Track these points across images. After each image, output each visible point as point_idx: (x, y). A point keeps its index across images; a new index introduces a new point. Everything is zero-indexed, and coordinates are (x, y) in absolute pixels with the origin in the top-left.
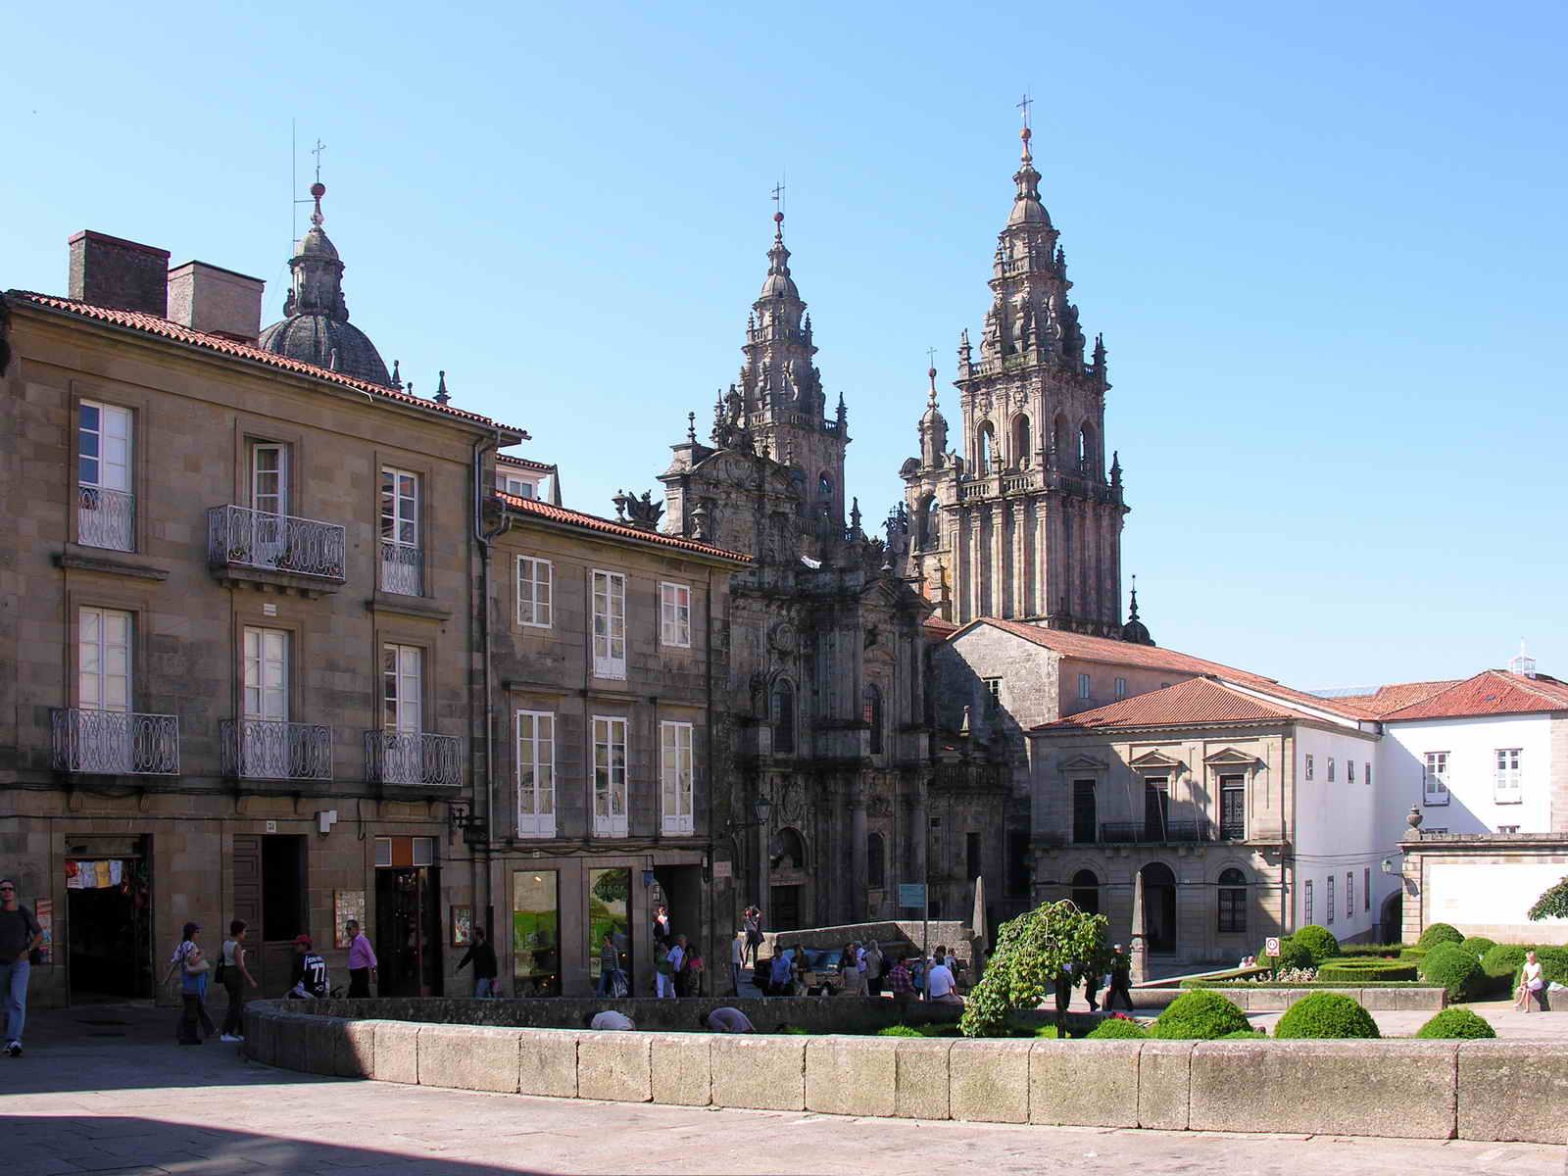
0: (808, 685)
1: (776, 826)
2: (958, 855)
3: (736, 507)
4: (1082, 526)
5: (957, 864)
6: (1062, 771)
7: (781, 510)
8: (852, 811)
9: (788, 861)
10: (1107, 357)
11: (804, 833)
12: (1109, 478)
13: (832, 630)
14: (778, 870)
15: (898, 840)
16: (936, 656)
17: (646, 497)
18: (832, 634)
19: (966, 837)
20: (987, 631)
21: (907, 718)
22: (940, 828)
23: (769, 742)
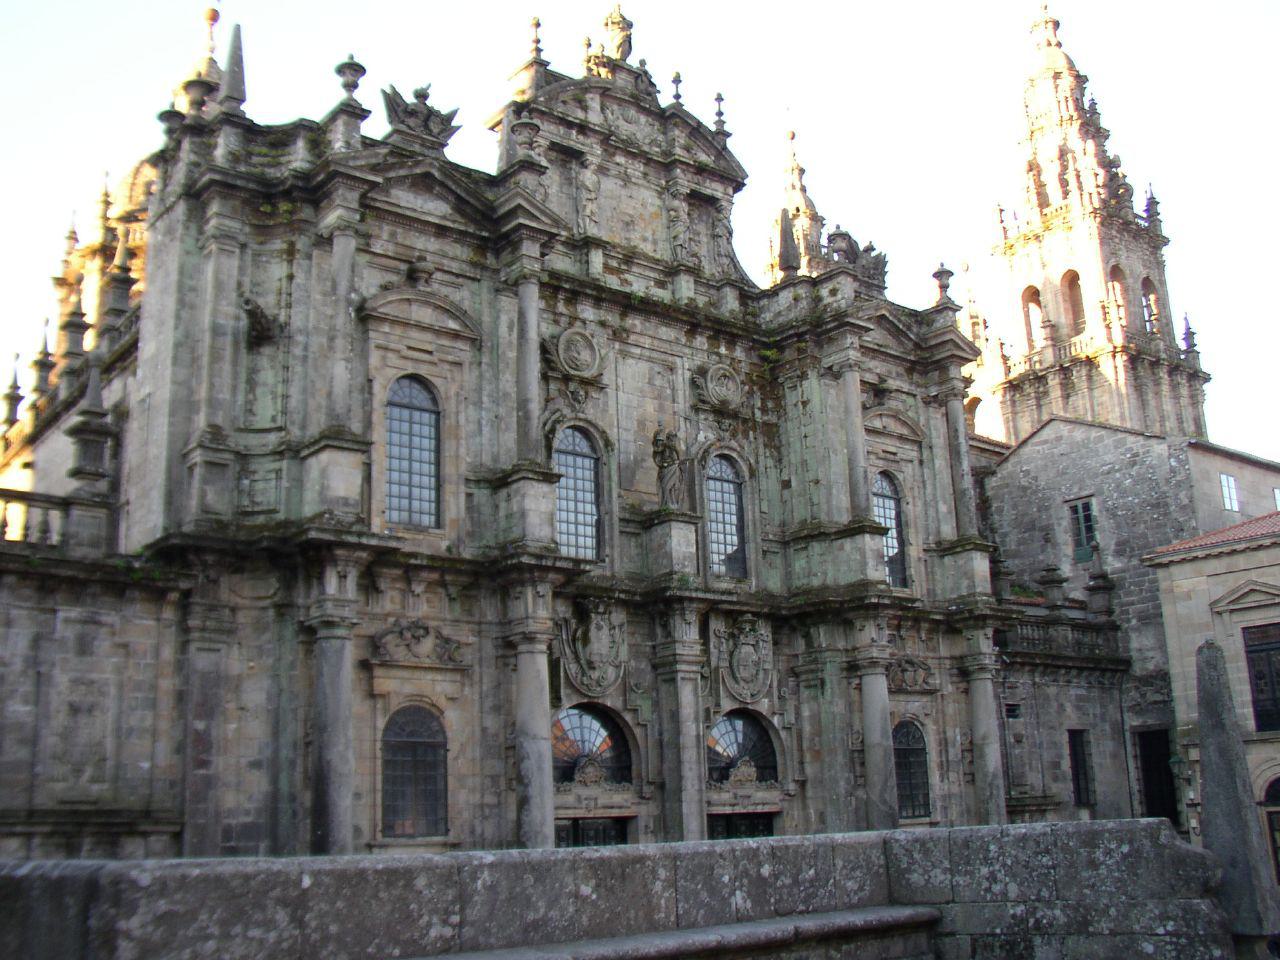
0: (773, 473)
1: (718, 705)
2: (1056, 765)
3: (626, 180)
4: (1157, 394)
5: (1056, 779)
6: (1219, 613)
7: (708, 192)
8: (860, 677)
9: (746, 770)
10: (1160, 208)
11: (776, 720)
12: (1182, 346)
13: (803, 376)
14: (727, 785)
15: (950, 734)
16: (991, 483)
17: (422, 95)
18: (805, 383)
19: (1065, 738)
20: (1065, 433)
21: (948, 531)
22: (1022, 720)
23: (694, 550)
